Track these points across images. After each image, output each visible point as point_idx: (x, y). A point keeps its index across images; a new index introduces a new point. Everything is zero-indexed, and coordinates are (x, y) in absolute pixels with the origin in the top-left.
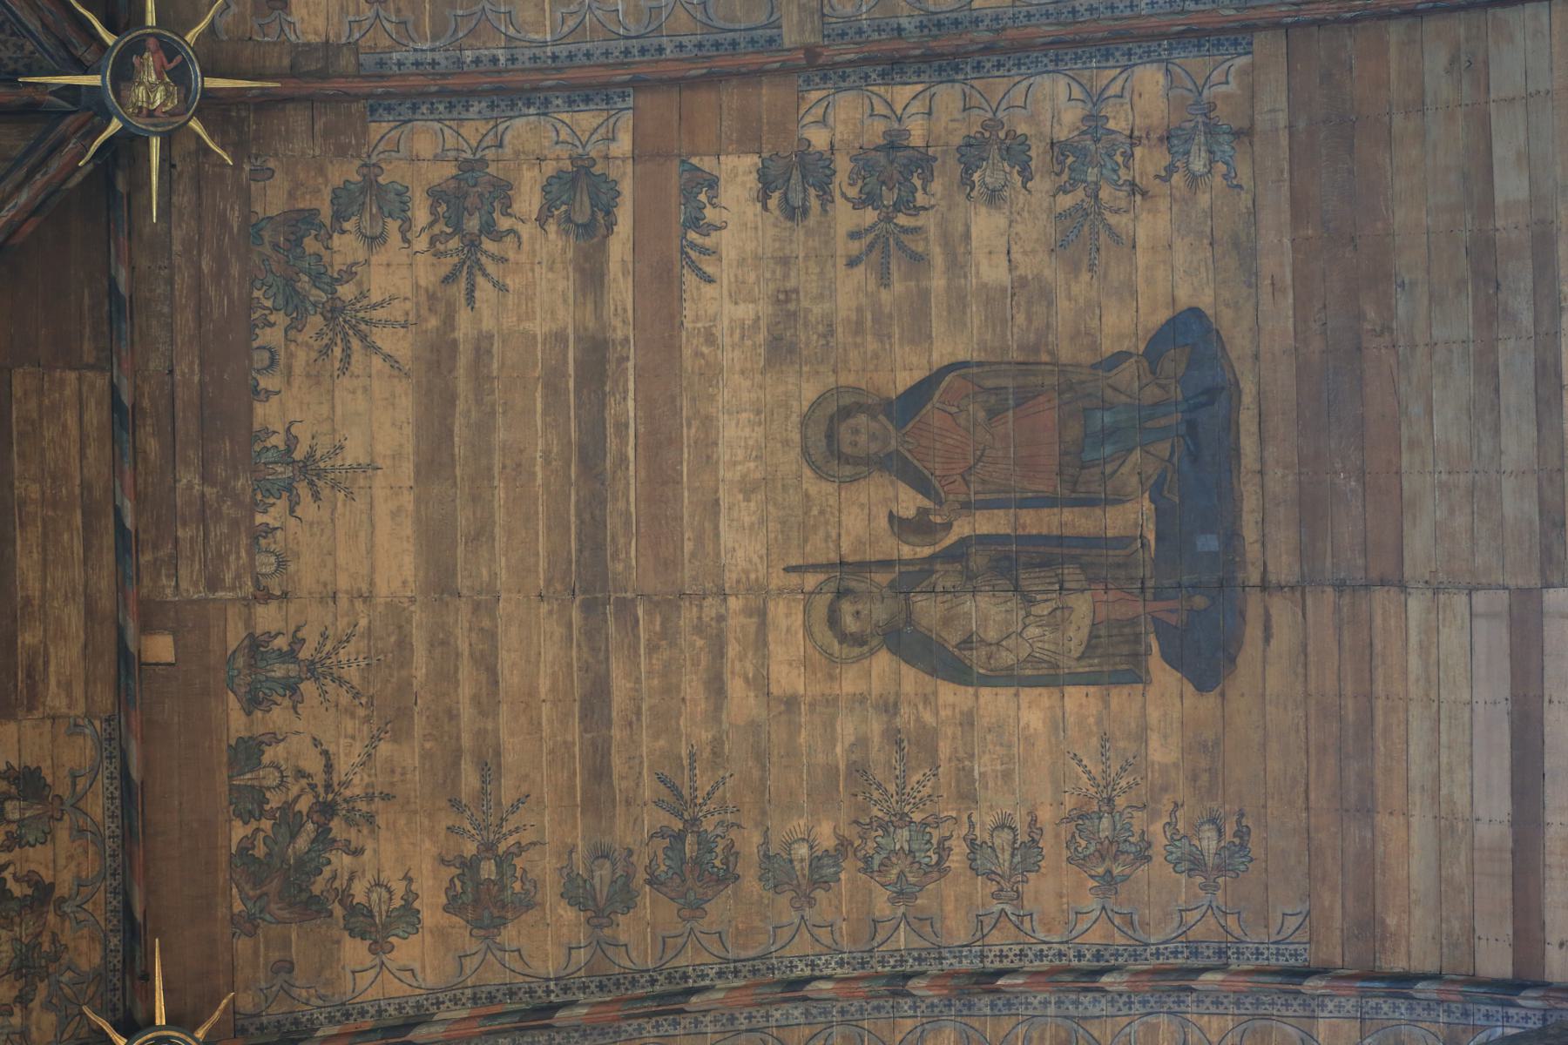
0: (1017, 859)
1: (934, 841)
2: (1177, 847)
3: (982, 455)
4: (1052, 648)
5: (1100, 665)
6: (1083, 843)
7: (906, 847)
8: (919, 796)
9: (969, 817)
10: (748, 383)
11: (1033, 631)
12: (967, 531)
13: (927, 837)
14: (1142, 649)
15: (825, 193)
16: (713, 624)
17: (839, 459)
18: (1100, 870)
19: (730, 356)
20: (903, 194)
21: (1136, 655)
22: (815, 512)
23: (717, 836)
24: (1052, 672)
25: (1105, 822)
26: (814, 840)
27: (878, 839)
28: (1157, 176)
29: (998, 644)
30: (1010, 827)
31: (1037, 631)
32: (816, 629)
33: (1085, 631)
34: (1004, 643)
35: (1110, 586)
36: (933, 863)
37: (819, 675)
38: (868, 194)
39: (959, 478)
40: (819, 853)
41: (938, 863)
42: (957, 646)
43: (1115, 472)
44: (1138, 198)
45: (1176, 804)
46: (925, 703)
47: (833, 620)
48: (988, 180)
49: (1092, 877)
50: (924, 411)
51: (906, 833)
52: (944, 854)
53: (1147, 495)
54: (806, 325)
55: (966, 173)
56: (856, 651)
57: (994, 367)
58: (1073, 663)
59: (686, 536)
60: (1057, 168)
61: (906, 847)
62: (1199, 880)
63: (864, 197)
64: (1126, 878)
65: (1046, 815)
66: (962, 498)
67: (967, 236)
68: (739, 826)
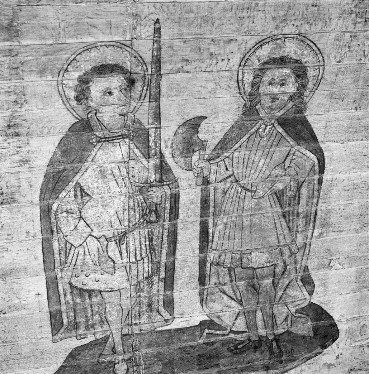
3: (247, 190)
4: (79, 263)
5: (67, 303)
11: (93, 245)
12: (183, 184)
14: (82, 331)
17: (260, 69)
21: (76, 326)
29: (81, 218)
32: (93, 53)
33: (95, 287)
34: (82, 222)
39: (230, 173)
42: (78, 183)
43: (225, 293)
46: (20, 161)
50: (289, 139)
53: (206, 318)
56: (72, 94)
57: (316, 193)
58: (66, 281)
66: (212, 178)
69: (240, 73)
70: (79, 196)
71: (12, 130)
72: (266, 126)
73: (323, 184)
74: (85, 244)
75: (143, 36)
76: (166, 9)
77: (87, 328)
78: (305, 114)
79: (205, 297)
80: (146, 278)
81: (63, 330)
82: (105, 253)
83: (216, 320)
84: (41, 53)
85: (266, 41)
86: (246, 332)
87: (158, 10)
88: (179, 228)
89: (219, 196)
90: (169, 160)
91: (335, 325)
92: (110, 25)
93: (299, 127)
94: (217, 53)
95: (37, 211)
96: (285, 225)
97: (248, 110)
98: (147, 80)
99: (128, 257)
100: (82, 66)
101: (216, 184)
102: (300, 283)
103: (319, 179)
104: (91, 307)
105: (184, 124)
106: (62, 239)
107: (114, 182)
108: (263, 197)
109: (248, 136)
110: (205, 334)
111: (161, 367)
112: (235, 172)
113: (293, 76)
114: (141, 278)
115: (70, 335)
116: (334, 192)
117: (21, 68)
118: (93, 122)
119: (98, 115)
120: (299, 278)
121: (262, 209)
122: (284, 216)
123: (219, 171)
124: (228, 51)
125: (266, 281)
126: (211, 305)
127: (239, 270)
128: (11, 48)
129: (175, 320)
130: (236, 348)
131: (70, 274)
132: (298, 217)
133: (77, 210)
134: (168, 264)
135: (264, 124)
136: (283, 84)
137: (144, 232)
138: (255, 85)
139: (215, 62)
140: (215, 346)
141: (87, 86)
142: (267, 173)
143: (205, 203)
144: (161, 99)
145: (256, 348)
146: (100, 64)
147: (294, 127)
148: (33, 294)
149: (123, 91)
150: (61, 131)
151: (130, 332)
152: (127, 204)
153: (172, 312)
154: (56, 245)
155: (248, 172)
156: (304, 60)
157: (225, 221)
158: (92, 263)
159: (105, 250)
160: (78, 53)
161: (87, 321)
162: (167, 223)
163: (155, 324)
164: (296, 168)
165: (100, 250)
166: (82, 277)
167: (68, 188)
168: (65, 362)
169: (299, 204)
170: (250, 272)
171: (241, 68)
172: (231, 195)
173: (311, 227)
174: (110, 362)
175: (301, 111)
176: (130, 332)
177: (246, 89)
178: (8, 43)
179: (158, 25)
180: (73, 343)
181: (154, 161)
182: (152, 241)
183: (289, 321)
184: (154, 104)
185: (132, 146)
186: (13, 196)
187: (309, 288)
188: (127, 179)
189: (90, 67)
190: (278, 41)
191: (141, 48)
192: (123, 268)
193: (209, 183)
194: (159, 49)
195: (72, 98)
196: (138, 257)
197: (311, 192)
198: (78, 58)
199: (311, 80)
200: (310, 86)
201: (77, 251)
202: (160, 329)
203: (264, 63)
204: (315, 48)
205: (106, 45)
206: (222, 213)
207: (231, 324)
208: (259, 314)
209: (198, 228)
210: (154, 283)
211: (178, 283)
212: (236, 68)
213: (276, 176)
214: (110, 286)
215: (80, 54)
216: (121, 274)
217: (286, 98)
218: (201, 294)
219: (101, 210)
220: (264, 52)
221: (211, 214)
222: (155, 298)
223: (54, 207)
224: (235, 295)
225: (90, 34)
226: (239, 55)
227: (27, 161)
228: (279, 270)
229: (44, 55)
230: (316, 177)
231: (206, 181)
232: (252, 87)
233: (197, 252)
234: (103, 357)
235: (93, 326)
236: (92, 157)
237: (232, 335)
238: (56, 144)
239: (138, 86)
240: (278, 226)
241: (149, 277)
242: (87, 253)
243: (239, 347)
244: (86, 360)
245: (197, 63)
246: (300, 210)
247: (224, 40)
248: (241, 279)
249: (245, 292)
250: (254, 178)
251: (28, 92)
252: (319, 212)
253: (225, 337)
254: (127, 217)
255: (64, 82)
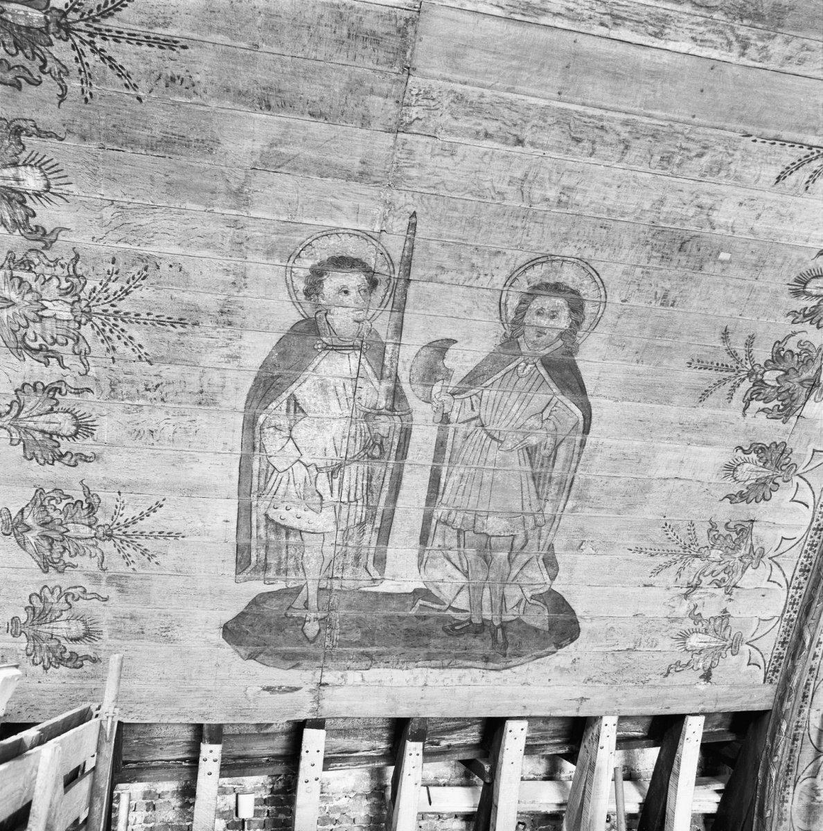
0: (39, 436)
1: (56, 347)
2: (59, 598)
3: (494, 438)
4: (281, 491)
5: (259, 537)
6: (61, 507)
7: (45, 313)
8: (114, 337)
9: (88, 390)
10: (647, 206)
11: (300, 472)
12: (417, 417)
13: (61, 339)
14: (271, 574)
15: (805, 316)
16: (361, 109)
17: (528, 294)
18: (29, 521)
19: (686, 188)
20: (768, 390)
21: (266, 568)
22: (476, 260)
23: (44, 61)
24: (255, 489)
25: (86, 531)
26: (48, 200)
27: (55, 282)
28: (696, 607)
29: (290, 437)
30: (77, 433)
31: (300, 479)
32: (333, 241)
33: (295, 524)
34: (291, 443)
35: (339, 548)
36: (28, 342)
37: (274, 237)
38: (783, 358)
39: (475, 414)
40: (29, 204)
41: (31, 349)
42: (293, 395)
44: (684, 590)
45: (106, 600)
46: (229, 356)
47: (342, 262)
48: (747, 465)
49: (22, 511)
50: (552, 385)
51: (66, 315)
52: (40, 356)
53: (422, 586)
54: (684, 279)
55: (761, 448)
56: (301, 286)
57: (576, 457)
58: (262, 511)
59: (487, 92)
60: (731, 525)
61: (45, 313)
62: (23, 617)
63: (782, 353)
64: (22, 545)
65: (90, 472)
66: (454, 416)
67: (707, 444)
68: (62, 98)
69: (504, 294)
70: (292, 411)
71: (225, 317)
72: (527, 364)
73: (586, 447)
74: (290, 470)
75: (395, 230)
76: (426, 202)
77: (278, 572)
78: (576, 358)
79: (425, 560)
80: (358, 525)
81: (249, 569)
82: (313, 486)
83: (434, 591)
84: (272, 231)
85: (540, 260)
86: (468, 611)
87: (416, 202)
88: (405, 470)
89: (459, 439)
90: (406, 387)
91: (577, 622)
92: (357, 210)
93: (567, 372)
94: (480, 265)
95: (240, 420)
96: (533, 488)
97: (508, 341)
98: (392, 284)
99: (340, 494)
100: (317, 254)
101: (457, 425)
102: (542, 564)
103: (582, 440)
104: (287, 547)
105: (429, 345)
106: (265, 459)
107: (336, 401)
108: (511, 450)
109: (503, 372)
110: (418, 605)
111: (359, 635)
112: (482, 414)
113: (567, 309)
114: (351, 523)
115: (257, 576)
116: (597, 459)
117: (246, 244)
118: (321, 324)
119: (328, 316)
120: (541, 557)
121: (509, 465)
122: (534, 479)
123: (462, 410)
124: (493, 265)
125: (500, 554)
126: (430, 571)
127: (469, 534)
128: (236, 218)
129: (385, 581)
130: (453, 629)
131: (268, 503)
132: (550, 482)
133: (287, 427)
134: (386, 512)
135: (524, 361)
136: (553, 317)
137: (363, 468)
138: (521, 312)
139: (475, 275)
140: (428, 622)
141: (320, 279)
142: (521, 422)
143: (440, 445)
144: (406, 310)
145: (477, 632)
146: (340, 255)
147: (561, 371)
148: (220, 520)
149: (362, 293)
150: (282, 328)
151: (329, 587)
152: (347, 430)
153: (382, 571)
154: (256, 465)
155: (498, 417)
156: (582, 292)
157: (462, 471)
158: (295, 494)
159: (313, 481)
160: (315, 237)
161: (279, 563)
162: (392, 461)
163: (360, 583)
164: (556, 422)
165: (308, 481)
166: (282, 510)
167: (280, 399)
168: (246, 608)
169: (553, 466)
170: (484, 539)
171: (505, 288)
172: (474, 441)
173: (564, 497)
174: (300, 618)
175: (571, 354)
176: (329, 587)
177: (509, 315)
178: (235, 212)
179: (414, 220)
180: (258, 587)
181: (387, 385)
182: (371, 480)
183: (522, 607)
184: (396, 315)
185: (363, 361)
186: (214, 397)
187: (551, 571)
188: (352, 400)
189: (327, 257)
190: (554, 264)
191: (390, 244)
192: (332, 508)
193: (449, 422)
194: (412, 248)
195: (301, 291)
196: (352, 498)
197: (570, 455)
198: (314, 243)
199: (587, 317)
200: (585, 325)
201: (279, 477)
202: (365, 589)
203: (534, 287)
204: (598, 280)
205: (349, 234)
206: (460, 461)
207: (451, 599)
208: (487, 592)
209: (428, 474)
210: (366, 532)
211: (394, 538)
212: (500, 287)
213: (531, 428)
214: (313, 527)
215: (317, 239)
216: (328, 513)
217: (555, 335)
218: (420, 556)
219: (316, 432)
220: (536, 274)
221: (447, 460)
222: (364, 551)
223: (261, 419)
224: (461, 564)
225: (331, 217)
226: (507, 273)
227: (237, 357)
228: (518, 542)
229: (275, 233)
230: (579, 438)
231: (446, 419)
232: (516, 314)
233: (423, 503)
234: (292, 610)
235: (286, 571)
236: (313, 366)
237: (450, 612)
238: (274, 344)
239: (381, 289)
240: (525, 489)
241: (361, 524)
242: (291, 481)
243: (457, 628)
244: (272, 607)
245: (454, 273)
246: (554, 475)
247: (490, 252)
248: (471, 546)
249: (473, 562)
250: (504, 425)
251: (250, 274)
252: (576, 480)
253: (442, 613)
254: (345, 446)
255: (293, 270)
